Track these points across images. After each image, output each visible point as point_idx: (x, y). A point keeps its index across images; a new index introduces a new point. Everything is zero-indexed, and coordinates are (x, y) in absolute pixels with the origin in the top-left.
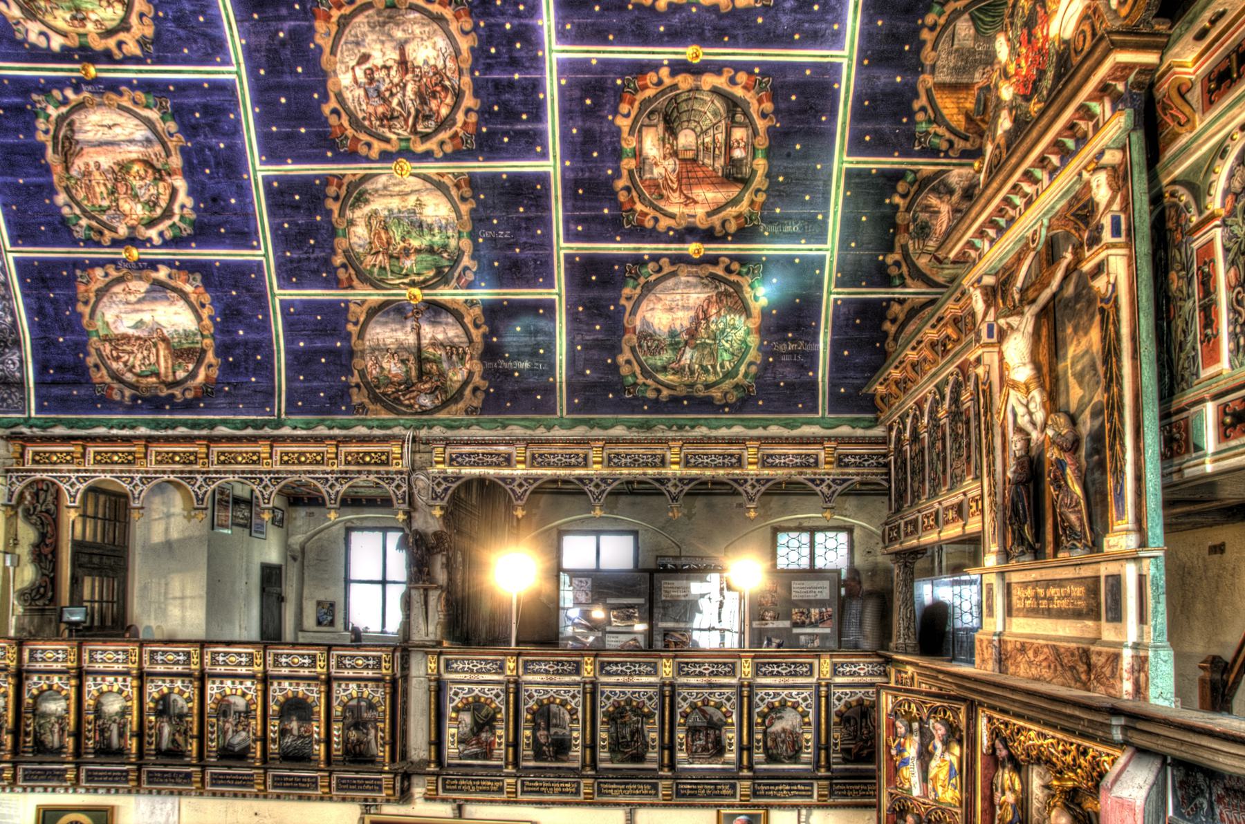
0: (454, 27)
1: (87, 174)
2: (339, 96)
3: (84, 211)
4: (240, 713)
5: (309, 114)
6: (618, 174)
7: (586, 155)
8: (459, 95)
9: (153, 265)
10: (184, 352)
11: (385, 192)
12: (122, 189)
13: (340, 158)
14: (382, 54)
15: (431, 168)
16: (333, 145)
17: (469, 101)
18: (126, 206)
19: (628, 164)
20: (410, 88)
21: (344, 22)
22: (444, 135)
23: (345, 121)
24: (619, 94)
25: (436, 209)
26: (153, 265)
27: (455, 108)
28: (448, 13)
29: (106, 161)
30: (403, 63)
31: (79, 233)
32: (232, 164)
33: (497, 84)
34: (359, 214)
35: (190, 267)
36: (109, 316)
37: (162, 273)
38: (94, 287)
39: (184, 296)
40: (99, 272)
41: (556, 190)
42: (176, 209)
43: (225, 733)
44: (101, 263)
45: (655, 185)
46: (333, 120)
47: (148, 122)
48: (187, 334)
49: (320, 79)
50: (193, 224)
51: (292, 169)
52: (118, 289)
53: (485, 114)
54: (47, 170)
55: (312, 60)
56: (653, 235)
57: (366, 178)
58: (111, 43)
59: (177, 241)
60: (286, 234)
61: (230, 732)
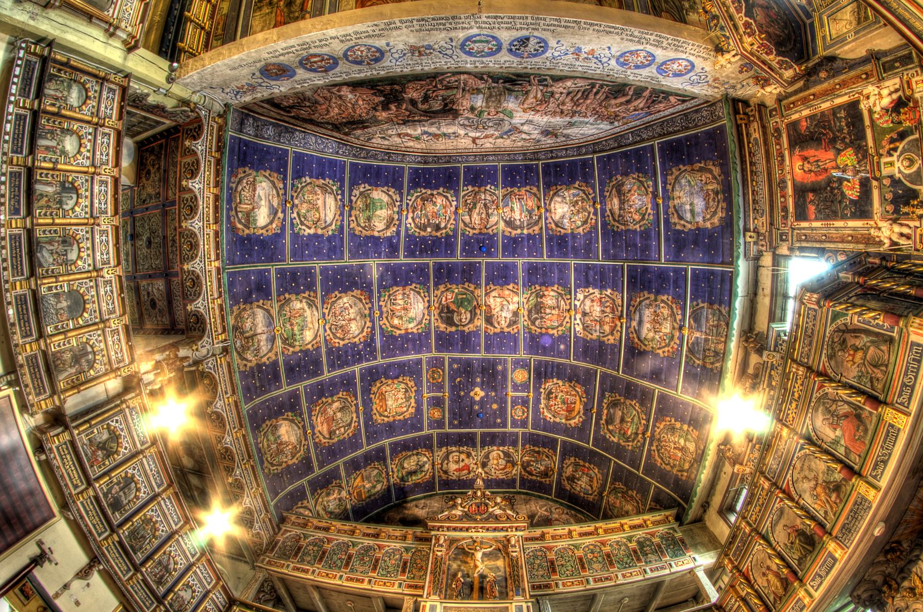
0: (361, 336)
2: (340, 298)
3: (303, 187)
4: (66, 255)
5: (335, 287)
6: (326, 397)
7: (331, 386)
8: (343, 339)
10: (249, 218)
11: (312, 315)
12: (311, 206)
13: (322, 296)
15: (321, 331)
16: (326, 294)
17: (342, 343)
18: (305, 205)
19: (330, 400)
20: (344, 322)
21: (361, 300)
22: (331, 336)
23: (334, 299)
24: (348, 391)
25: (309, 335)
26: (284, 211)
27: (340, 338)
28: (364, 334)
29: (320, 203)
30: (350, 320)
31: (296, 182)
32: (318, 254)
33: (347, 352)
35: (283, 228)
36: (264, 184)
37: (280, 215)
38: (276, 181)
39: (271, 222)
40: (281, 186)
41: (320, 378)
42: (303, 227)
43: (50, 242)
44: (285, 188)
45: (325, 410)
46: (333, 295)
47: (331, 224)
48: (255, 220)
49: (345, 290)
50: (298, 233)
52: (275, 192)
53: (339, 349)
54: (318, 178)
56: (310, 416)
58: (353, 218)
59: (292, 224)
60: (296, 274)
61: (51, 248)
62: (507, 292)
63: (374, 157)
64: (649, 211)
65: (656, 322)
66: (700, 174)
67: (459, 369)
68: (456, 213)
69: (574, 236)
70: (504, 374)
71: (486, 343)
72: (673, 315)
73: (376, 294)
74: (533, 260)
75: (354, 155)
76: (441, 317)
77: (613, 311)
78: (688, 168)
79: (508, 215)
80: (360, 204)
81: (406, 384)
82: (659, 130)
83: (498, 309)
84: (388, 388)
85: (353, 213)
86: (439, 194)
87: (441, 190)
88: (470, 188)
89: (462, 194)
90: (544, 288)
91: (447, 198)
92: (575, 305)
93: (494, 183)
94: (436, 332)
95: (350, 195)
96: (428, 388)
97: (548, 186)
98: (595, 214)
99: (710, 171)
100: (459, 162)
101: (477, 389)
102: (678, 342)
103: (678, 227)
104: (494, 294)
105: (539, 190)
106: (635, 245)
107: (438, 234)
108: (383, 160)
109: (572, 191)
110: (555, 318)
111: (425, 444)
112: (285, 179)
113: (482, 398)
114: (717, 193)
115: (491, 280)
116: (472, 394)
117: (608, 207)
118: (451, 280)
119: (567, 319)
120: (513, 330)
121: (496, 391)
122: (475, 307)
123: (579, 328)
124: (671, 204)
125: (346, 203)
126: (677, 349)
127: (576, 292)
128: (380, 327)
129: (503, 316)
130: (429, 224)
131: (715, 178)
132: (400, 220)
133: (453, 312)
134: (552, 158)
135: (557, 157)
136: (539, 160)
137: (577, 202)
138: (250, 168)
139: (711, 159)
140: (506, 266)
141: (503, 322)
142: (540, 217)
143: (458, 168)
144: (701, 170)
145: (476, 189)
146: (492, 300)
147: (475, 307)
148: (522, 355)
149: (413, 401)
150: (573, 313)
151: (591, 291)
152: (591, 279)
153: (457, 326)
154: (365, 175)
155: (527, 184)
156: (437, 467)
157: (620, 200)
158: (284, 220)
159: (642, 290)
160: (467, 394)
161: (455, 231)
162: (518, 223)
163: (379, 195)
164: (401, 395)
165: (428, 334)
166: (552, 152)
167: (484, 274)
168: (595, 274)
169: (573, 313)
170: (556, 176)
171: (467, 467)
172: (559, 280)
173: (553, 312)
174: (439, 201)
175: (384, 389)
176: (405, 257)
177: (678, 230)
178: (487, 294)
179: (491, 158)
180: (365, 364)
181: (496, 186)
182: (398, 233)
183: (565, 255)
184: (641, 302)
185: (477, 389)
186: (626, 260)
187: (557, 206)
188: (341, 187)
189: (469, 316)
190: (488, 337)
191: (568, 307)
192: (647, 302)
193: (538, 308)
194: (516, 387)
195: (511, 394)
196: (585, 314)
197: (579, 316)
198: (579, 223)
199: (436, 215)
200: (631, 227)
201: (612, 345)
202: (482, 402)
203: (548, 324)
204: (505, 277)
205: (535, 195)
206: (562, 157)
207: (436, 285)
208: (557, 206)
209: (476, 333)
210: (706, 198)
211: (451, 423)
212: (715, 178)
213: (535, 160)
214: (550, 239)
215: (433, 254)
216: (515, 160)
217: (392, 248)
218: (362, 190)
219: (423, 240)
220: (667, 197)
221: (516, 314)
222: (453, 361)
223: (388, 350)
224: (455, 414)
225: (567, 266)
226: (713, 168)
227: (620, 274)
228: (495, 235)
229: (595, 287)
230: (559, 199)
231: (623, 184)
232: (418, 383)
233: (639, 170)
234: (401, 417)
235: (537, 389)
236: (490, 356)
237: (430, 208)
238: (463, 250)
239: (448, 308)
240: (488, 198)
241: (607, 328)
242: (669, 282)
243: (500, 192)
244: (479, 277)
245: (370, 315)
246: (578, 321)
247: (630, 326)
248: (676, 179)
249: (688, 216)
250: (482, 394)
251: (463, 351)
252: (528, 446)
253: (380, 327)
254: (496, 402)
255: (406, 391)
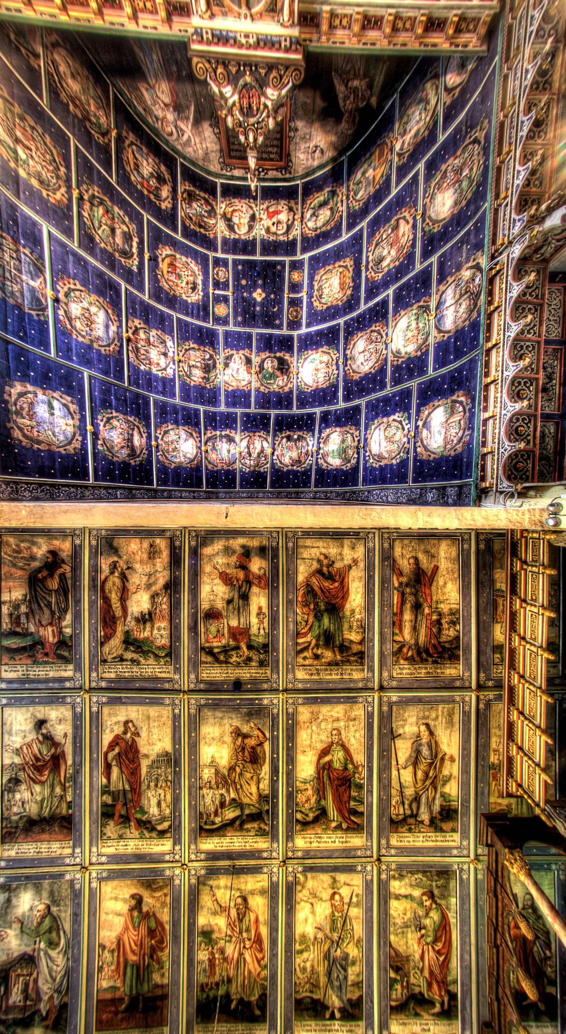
1: (387, 451)
9: (417, 427)
14: (361, 359)
17: (373, 328)
21: (354, 372)
28: (352, 343)
29: (384, 444)
31: (405, 456)
34: (403, 351)
37: (420, 423)
38: (424, 452)
40: (419, 450)
44: (415, 448)
51: (388, 380)
52: (425, 442)
53: (376, 322)
55: (362, 379)
57: (392, 353)
62: (234, 384)
63: (338, 494)
64: (102, 424)
65: (90, 322)
66: (41, 438)
67: (274, 320)
68: (274, 449)
69: (176, 423)
70: (236, 314)
71: (251, 342)
72: (70, 319)
73: (341, 379)
74: (212, 409)
75: (354, 493)
76: (288, 365)
77: (137, 350)
78: (54, 448)
79: (232, 446)
80: (350, 452)
81: (320, 303)
82: (87, 493)
83: (241, 371)
84: (336, 296)
85: (356, 443)
86: (287, 466)
87: (285, 469)
88: (262, 470)
89: (268, 465)
90: (203, 384)
91: (281, 462)
92: (174, 364)
93: (243, 474)
94: (293, 353)
95: (358, 458)
96: (301, 302)
97: (198, 468)
98: (157, 438)
99: (24, 435)
100: (270, 492)
101: (259, 299)
102: (59, 288)
103: (69, 399)
104: (244, 383)
105: (206, 466)
106: (117, 399)
107: (288, 433)
108: (331, 492)
109: (178, 460)
110: (192, 358)
111: (308, 243)
112: (415, 458)
113: (255, 291)
114: (18, 413)
115: (247, 395)
116: (264, 295)
117: (144, 440)
118: (278, 395)
119: (181, 354)
120: (229, 352)
121: (243, 297)
122: (260, 372)
123: (169, 344)
124: (78, 423)
125: (362, 451)
126: (58, 279)
127: (174, 375)
128: (338, 351)
129: (237, 363)
130: (295, 441)
131: (21, 429)
132: (319, 443)
133: (278, 369)
134: (194, 492)
135: (190, 492)
136: (205, 492)
137: (174, 450)
138: (450, 456)
139: (24, 447)
140: (234, 405)
141: (237, 359)
142: (206, 443)
143: (272, 487)
144: (39, 442)
145: (257, 469)
146: (247, 379)
147: (260, 372)
148: (221, 329)
149: (316, 287)
150: (176, 358)
151: (160, 373)
152: (160, 383)
153: (275, 357)
154: (346, 478)
155: (217, 472)
156: (298, 216)
157: (132, 442)
158: (417, 421)
159: (106, 356)
160: (268, 296)
161: (275, 435)
162: (224, 440)
163: (335, 462)
164: (326, 291)
165: (300, 350)
166: (194, 498)
167: (253, 399)
168: (156, 387)
169: (176, 358)
170: (191, 475)
171: (271, 215)
172: (189, 389)
173: (194, 363)
174: (287, 460)
175: (341, 295)
176: (315, 413)
177: (69, 395)
178: (250, 383)
179: (245, 495)
180: (354, 314)
181: (241, 471)
182: (320, 432)
183: (184, 408)
184: (109, 345)
185: (259, 299)
186: (126, 390)
187: (191, 451)
188: (366, 462)
189: (265, 366)
190: (250, 347)
191: (181, 364)
192: (100, 343)
193: (208, 368)
194: (225, 299)
195: (229, 293)
196: (165, 355)
197: (170, 354)
198: (172, 433)
199: (290, 449)
200: (121, 416)
201: (136, 318)
202: (254, 287)
203: (198, 354)
204: (235, 396)
205: (210, 462)
206: (186, 491)
207: (291, 392)
208: (191, 451)
209: (259, 350)
210: (32, 415)
211: (284, 267)
212: (21, 429)
213: (208, 492)
214: (197, 424)
215: (292, 417)
216: (226, 493)
217: (326, 420)
218: (349, 465)
219: (300, 428)
220: (82, 429)
221: (226, 365)
222: (280, 327)
223: (334, 331)
224: (279, 276)
225: (182, 399)
226: (21, 438)
227: (132, 378)
228: (242, 431)
229: (156, 376)
230: (189, 455)
231: (129, 455)
232: (310, 304)
233: (112, 463)
234: (327, 268)
235: (206, 295)
236: (248, 330)
237: (294, 455)
238: (269, 419)
239: (282, 373)
240: (248, 462)
241: (142, 335)
242: (77, 353)
243: (238, 466)
244: (256, 397)
245: (347, 360)
246: (171, 350)
247: (118, 327)
248: (70, 443)
249: (56, 404)
250: (255, 295)
251: (271, 335)
252: (212, 236)
253: (338, 351)
254: (243, 287)
255: (321, 296)
